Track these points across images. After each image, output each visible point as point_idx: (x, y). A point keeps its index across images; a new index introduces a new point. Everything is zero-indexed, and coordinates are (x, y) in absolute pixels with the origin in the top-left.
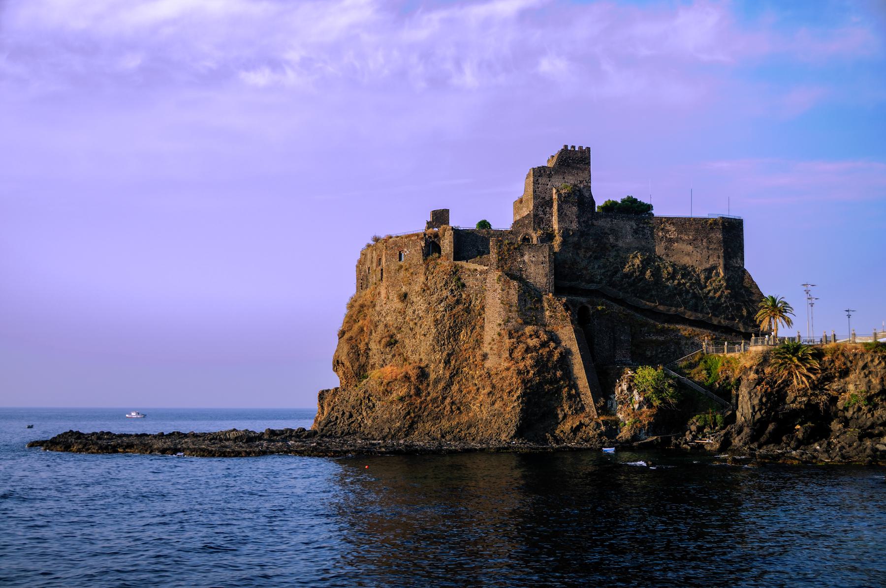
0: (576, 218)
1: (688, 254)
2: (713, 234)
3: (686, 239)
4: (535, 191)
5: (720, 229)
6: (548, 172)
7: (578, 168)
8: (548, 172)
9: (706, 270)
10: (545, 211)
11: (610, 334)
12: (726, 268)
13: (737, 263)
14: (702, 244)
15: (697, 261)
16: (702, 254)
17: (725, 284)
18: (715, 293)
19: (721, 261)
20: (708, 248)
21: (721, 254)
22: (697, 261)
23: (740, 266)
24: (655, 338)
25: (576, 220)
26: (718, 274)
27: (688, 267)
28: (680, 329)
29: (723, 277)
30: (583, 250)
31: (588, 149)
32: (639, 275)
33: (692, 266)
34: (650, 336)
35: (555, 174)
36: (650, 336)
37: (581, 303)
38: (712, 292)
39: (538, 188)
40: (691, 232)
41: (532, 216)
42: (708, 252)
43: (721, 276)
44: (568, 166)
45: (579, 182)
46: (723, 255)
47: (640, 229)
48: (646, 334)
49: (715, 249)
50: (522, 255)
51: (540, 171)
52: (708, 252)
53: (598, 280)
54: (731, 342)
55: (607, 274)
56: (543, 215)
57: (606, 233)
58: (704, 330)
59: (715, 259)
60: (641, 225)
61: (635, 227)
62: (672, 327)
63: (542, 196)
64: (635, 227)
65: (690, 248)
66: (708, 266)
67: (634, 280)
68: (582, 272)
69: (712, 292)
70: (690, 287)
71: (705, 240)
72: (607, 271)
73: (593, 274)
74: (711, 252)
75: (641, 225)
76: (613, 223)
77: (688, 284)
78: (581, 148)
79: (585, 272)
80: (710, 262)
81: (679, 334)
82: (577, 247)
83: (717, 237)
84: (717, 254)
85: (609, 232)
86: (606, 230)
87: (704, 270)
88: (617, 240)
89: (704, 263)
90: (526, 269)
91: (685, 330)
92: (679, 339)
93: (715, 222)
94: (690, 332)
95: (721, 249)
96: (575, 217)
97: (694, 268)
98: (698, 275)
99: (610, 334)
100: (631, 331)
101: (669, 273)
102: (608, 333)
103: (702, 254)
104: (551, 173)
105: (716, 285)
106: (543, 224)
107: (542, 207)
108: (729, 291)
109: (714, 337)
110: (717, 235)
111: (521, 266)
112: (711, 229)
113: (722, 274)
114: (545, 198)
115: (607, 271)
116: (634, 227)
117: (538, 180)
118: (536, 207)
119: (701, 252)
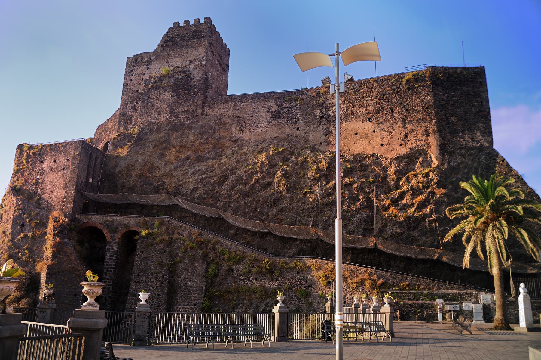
0: (168, 107)
1: (366, 137)
2: (414, 98)
3: (362, 113)
4: (125, 85)
5: (428, 87)
6: (146, 59)
7: (188, 46)
8: (146, 59)
9: (399, 158)
10: (136, 107)
11: (163, 276)
12: (443, 149)
13: (473, 140)
14: (393, 116)
15: (382, 145)
16: (391, 132)
17: (436, 179)
18: (413, 196)
19: (433, 140)
20: (404, 121)
21: (432, 126)
22: (382, 145)
23: (482, 146)
24: (258, 285)
25: (167, 109)
26: (427, 163)
27: (366, 157)
28: (309, 267)
29: (438, 166)
30: (174, 149)
31: (208, 20)
32: (263, 178)
33: (373, 155)
34: (249, 280)
35: (156, 59)
36: (249, 280)
37: (126, 226)
38: (408, 195)
39: (131, 80)
40: (371, 100)
41: (118, 117)
42: (405, 128)
43: (434, 166)
44: (175, 45)
45: (188, 62)
46: (436, 129)
47: (285, 110)
48: (242, 277)
49: (419, 121)
50: (42, 162)
51: (136, 60)
52: (405, 128)
53: (189, 191)
54: (426, 292)
55: (209, 181)
56: (133, 112)
57: (225, 124)
58: (359, 268)
59: (419, 137)
60: (286, 105)
61: (274, 108)
62: (525, 266)
63: (135, 88)
64: (274, 108)
65: (369, 126)
66: (404, 151)
67: (254, 185)
68: (164, 180)
69: (408, 195)
70: (361, 189)
71: (397, 110)
72: (210, 177)
73: (181, 183)
74: (409, 127)
75: (286, 105)
76: (238, 108)
77: (355, 185)
78: (197, 21)
79: (167, 180)
80: (410, 143)
81: (310, 277)
82: (164, 145)
83: (422, 101)
84: (424, 129)
85: (230, 121)
86: (226, 120)
87: (397, 159)
88: (242, 131)
89: (396, 147)
90: (43, 180)
91: (318, 269)
92: (309, 286)
93: (417, 78)
94: (327, 273)
95: (432, 120)
96: (166, 106)
97: (377, 159)
98: (385, 169)
99: (163, 276)
100: (207, 271)
101: (319, 170)
102: (160, 275)
103: (391, 132)
104: (151, 59)
105: (418, 183)
106: (131, 123)
107: (132, 103)
108: (444, 191)
109: (380, 281)
110: (423, 97)
111: (38, 177)
112: (408, 89)
113: (436, 163)
114: (137, 91)
115: (210, 177)
116: (273, 110)
117: (132, 71)
118: (124, 104)
119: (390, 129)
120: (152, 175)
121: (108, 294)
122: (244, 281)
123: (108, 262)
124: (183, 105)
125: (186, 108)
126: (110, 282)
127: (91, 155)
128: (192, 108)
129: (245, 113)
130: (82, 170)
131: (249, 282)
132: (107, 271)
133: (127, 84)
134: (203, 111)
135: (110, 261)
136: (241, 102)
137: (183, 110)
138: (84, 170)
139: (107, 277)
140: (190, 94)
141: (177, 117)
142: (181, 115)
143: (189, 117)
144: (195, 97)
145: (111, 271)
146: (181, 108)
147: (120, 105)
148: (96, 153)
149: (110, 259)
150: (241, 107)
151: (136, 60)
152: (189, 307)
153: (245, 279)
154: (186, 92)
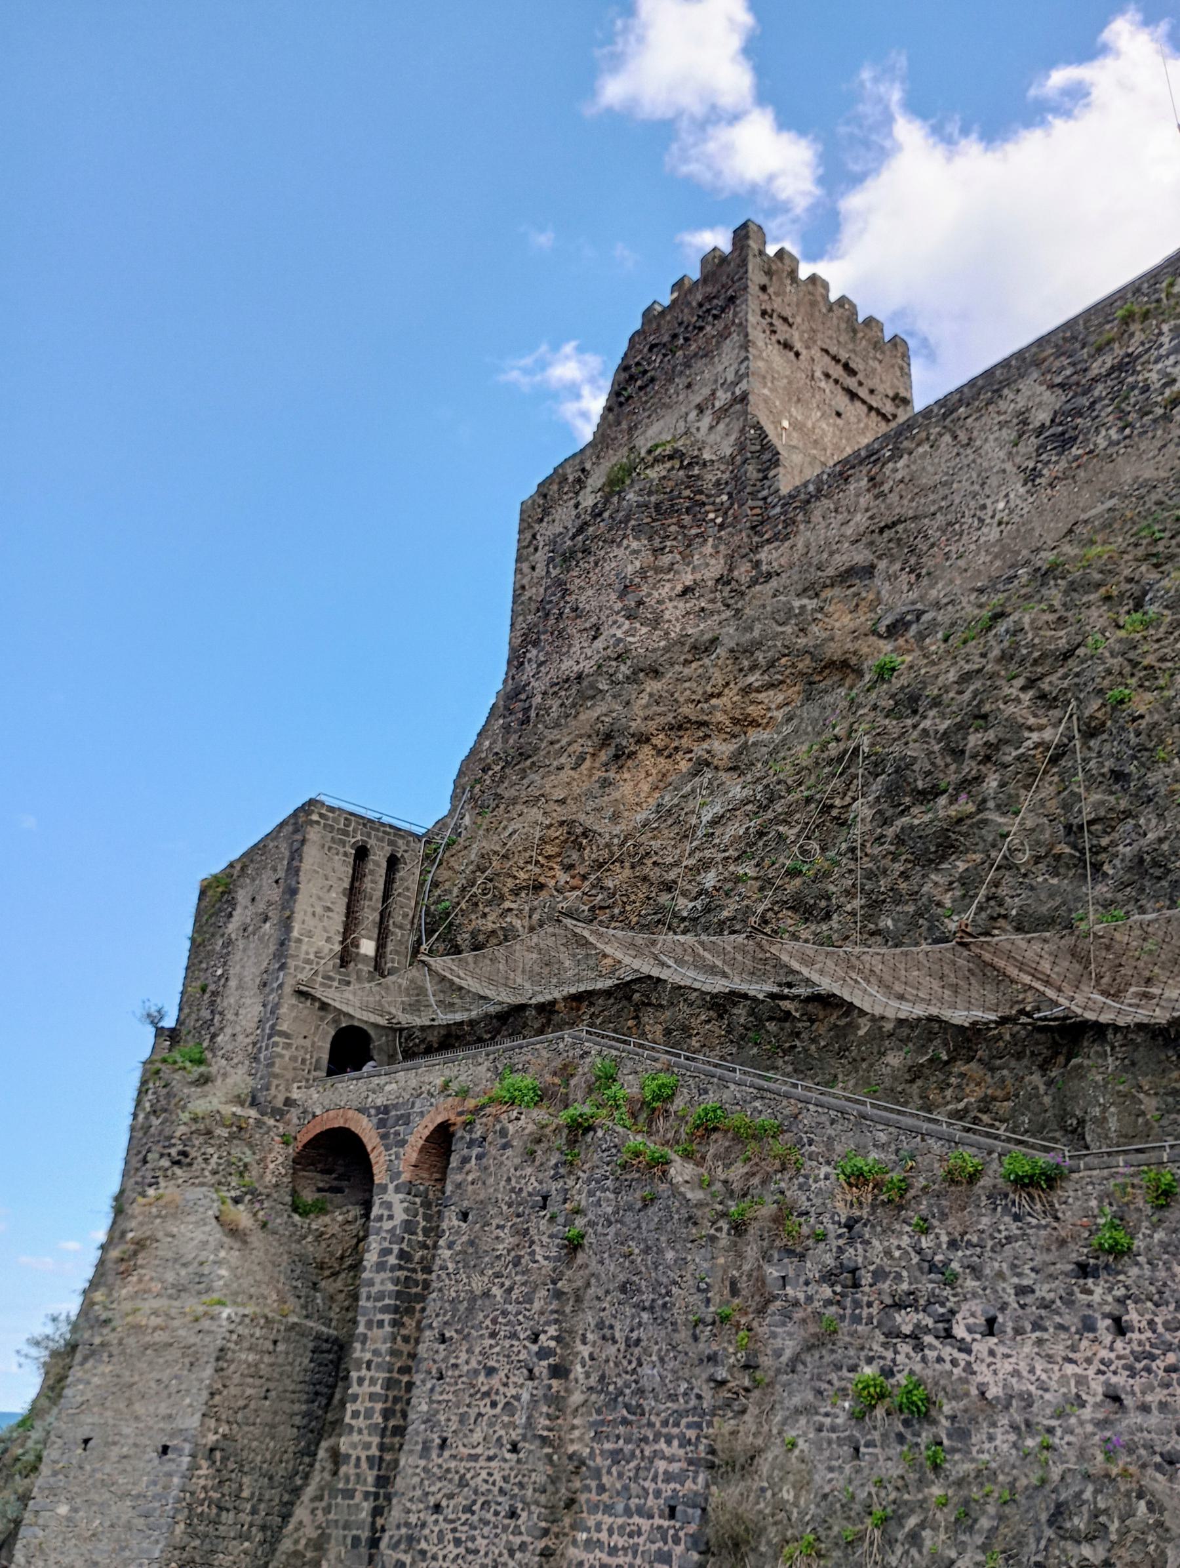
39: (533, 568)
76: (886, 488)
116: (1042, 416)
120: (573, 877)
121: (367, 1446)
122: (919, 1347)
123: (371, 1283)
124: (676, 572)
125: (688, 579)
126: (373, 1382)
127: (362, 853)
128: (717, 567)
129: (923, 491)
130: (319, 910)
131: (948, 1352)
132: (369, 1324)
133: (523, 587)
134: (757, 564)
135: (378, 1278)
136: (896, 455)
137: (679, 588)
138: (329, 909)
139: (368, 1356)
140: (700, 521)
141: (656, 622)
142: (673, 611)
143: (703, 610)
144: (722, 527)
145: (381, 1324)
146: (668, 585)
147: (504, 668)
148: (391, 843)
149: (380, 1267)
150: (899, 476)
151: (545, 496)
152: (645, 1524)
153: (927, 1330)
154: (687, 519)
